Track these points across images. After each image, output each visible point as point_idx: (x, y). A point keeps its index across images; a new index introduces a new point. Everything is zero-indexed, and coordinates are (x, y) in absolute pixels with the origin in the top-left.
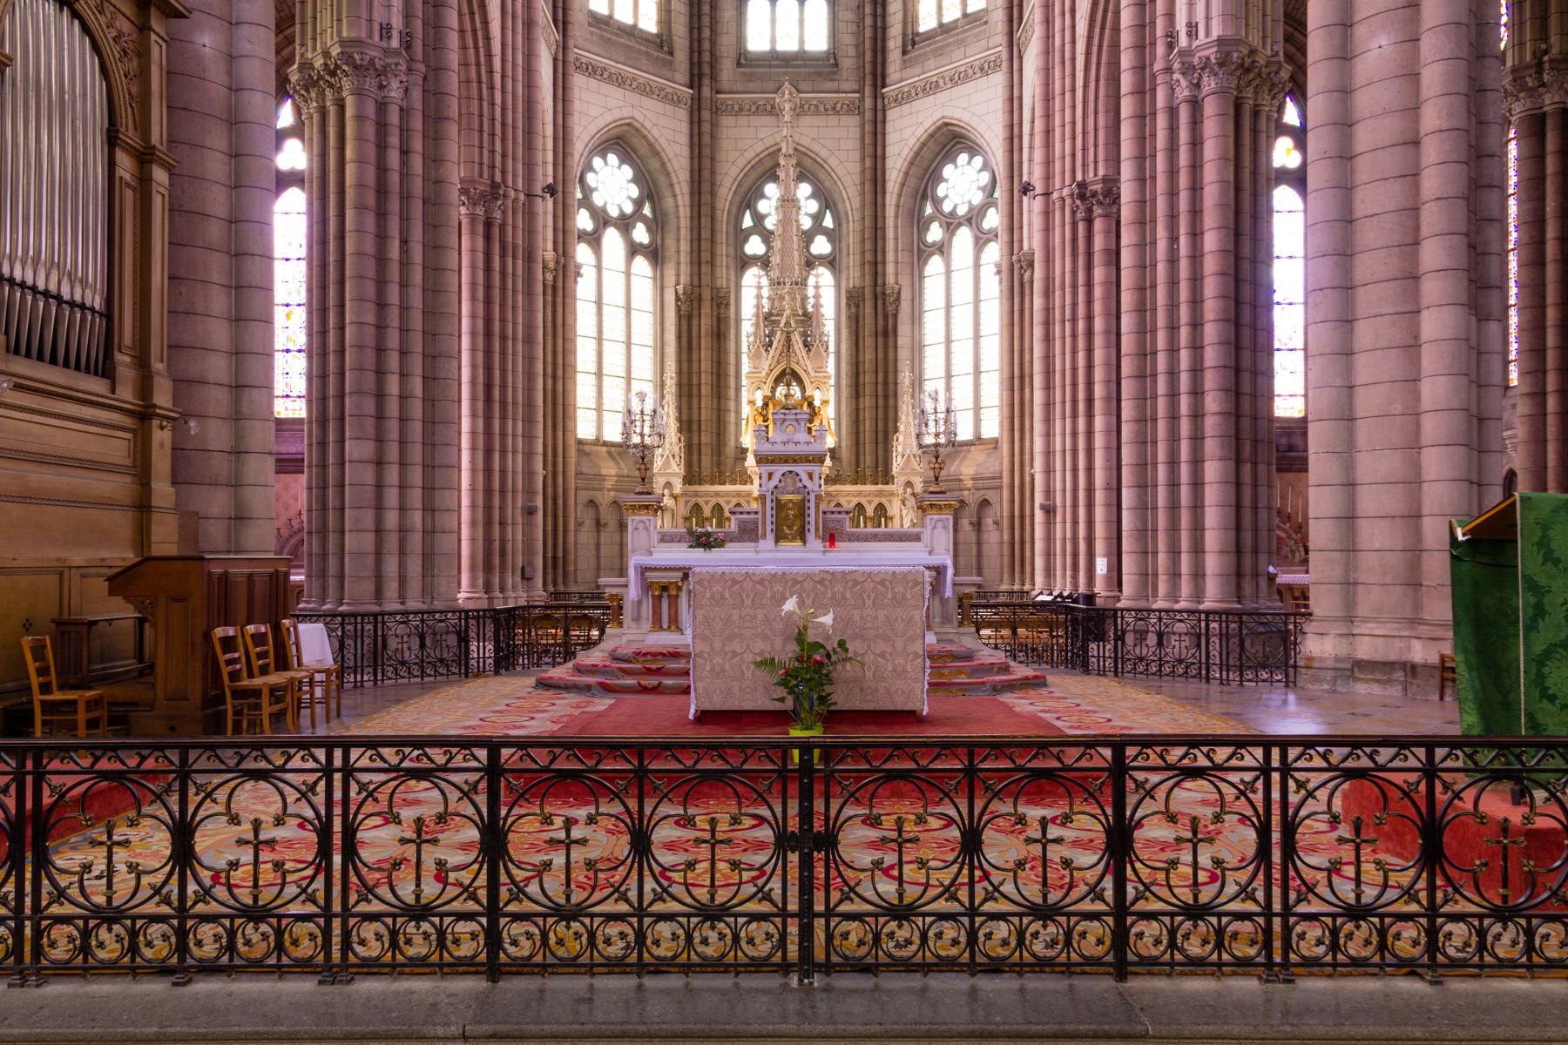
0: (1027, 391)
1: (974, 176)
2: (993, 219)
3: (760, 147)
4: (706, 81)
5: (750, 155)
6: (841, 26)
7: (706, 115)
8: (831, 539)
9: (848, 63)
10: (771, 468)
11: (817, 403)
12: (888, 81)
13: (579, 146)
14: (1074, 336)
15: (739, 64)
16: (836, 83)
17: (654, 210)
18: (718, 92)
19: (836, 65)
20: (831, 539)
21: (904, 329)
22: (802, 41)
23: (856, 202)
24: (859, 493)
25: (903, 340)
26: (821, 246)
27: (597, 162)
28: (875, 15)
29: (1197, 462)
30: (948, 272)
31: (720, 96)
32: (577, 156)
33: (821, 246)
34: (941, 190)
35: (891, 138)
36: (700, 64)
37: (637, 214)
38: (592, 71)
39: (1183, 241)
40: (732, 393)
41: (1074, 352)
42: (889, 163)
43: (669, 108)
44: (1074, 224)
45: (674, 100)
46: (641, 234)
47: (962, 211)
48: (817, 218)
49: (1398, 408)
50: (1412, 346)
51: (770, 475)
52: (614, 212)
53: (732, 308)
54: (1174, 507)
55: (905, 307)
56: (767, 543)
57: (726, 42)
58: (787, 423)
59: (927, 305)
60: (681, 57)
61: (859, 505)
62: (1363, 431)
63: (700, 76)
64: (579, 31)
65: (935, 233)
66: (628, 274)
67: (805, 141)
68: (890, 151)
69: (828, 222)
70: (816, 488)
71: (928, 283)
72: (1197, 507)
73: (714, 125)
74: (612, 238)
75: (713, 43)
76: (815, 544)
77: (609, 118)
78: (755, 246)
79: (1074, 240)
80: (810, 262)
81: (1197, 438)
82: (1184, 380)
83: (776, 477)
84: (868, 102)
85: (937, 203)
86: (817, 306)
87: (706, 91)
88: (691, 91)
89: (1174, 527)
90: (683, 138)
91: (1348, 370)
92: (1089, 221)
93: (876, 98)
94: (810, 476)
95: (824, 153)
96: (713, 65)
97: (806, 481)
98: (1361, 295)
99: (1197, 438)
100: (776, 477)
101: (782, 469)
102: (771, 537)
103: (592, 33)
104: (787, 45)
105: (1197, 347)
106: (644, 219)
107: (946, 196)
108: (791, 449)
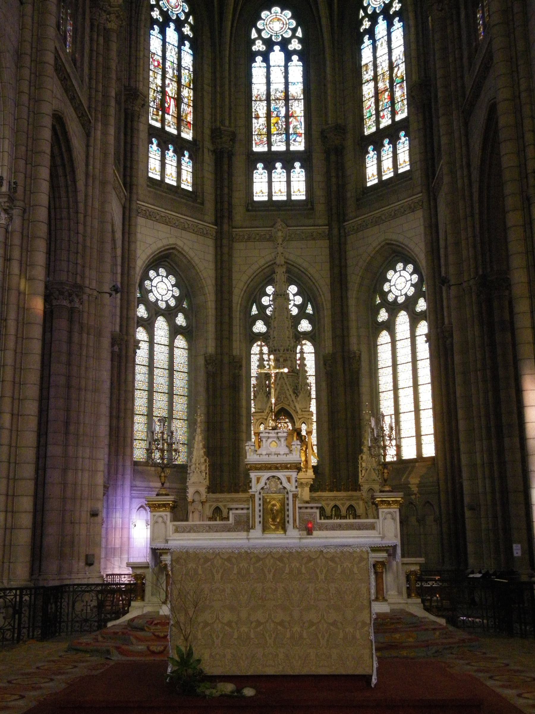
1: (408, 277)
2: (422, 305)
3: (262, 262)
4: (226, 220)
5: (255, 267)
6: (315, 185)
7: (225, 241)
9: (320, 208)
10: (259, 474)
11: (304, 433)
12: (347, 218)
13: (140, 263)
15: (248, 210)
16: (311, 221)
17: (190, 304)
18: (233, 228)
19: (312, 209)
21: (365, 382)
22: (289, 194)
23: (328, 296)
24: (335, 498)
25: (365, 389)
26: (305, 326)
27: (152, 274)
28: (337, 177)
30: (394, 342)
31: (234, 230)
32: (138, 269)
33: (305, 326)
34: (386, 287)
35: (351, 254)
36: (222, 210)
37: (178, 308)
38: (149, 216)
40: (244, 427)
42: (350, 270)
43: (201, 238)
45: (204, 235)
46: (180, 320)
47: (401, 300)
48: (302, 308)
52: (162, 305)
53: (244, 369)
55: (364, 365)
56: (257, 532)
57: (238, 197)
58: (270, 440)
59: (381, 364)
60: (210, 206)
61: (335, 506)
63: (222, 217)
64: (142, 190)
65: (383, 316)
66: (171, 347)
67: (292, 257)
68: (350, 262)
69: (309, 310)
70: (294, 489)
71: (380, 349)
73: (231, 248)
74: (161, 324)
75: (230, 197)
77: (160, 244)
78: (260, 327)
80: (299, 337)
83: (263, 481)
84: (335, 232)
85: (384, 295)
86: (303, 365)
87: (226, 227)
88: (216, 227)
90: (210, 257)
93: (339, 230)
95: (305, 265)
96: (230, 212)
97: (285, 484)
103: (149, 192)
104: (280, 196)
106: (183, 311)
107: (390, 291)
108: (274, 459)
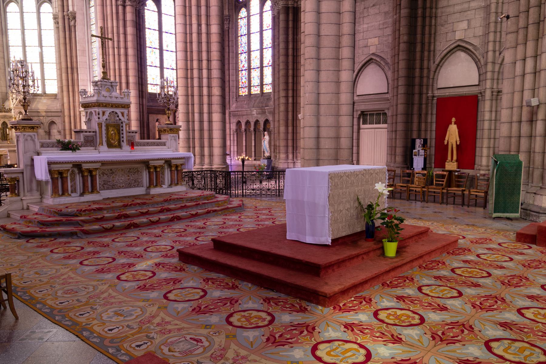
0: (75, 75)
8: (132, 145)
10: (104, 109)
14: (119, 55)
20: (132, 145)
29: (210, 113)
30: (22, 13)
39: (204, 27)
41: (119, 62)
44: (117, 6)
49: (333, 102)
50: (338, 82)
51: (104, 113)
54: (201, 130)
62: (323, 109)
70: (126, 121)
72: (210, 130)
76: (126, 147)
79: (117, 13)
81: (210, 104)
82: (205, 81)
83: (107, 114)
89: (202, 138)
91: (318, 88)
92: (124, 7)
94: (123, 114)
98: (323, 62)
99: (210, 104)
100: (107, 114)
101: (108, 111)
102: (105, 143)
105: (209, 70)
